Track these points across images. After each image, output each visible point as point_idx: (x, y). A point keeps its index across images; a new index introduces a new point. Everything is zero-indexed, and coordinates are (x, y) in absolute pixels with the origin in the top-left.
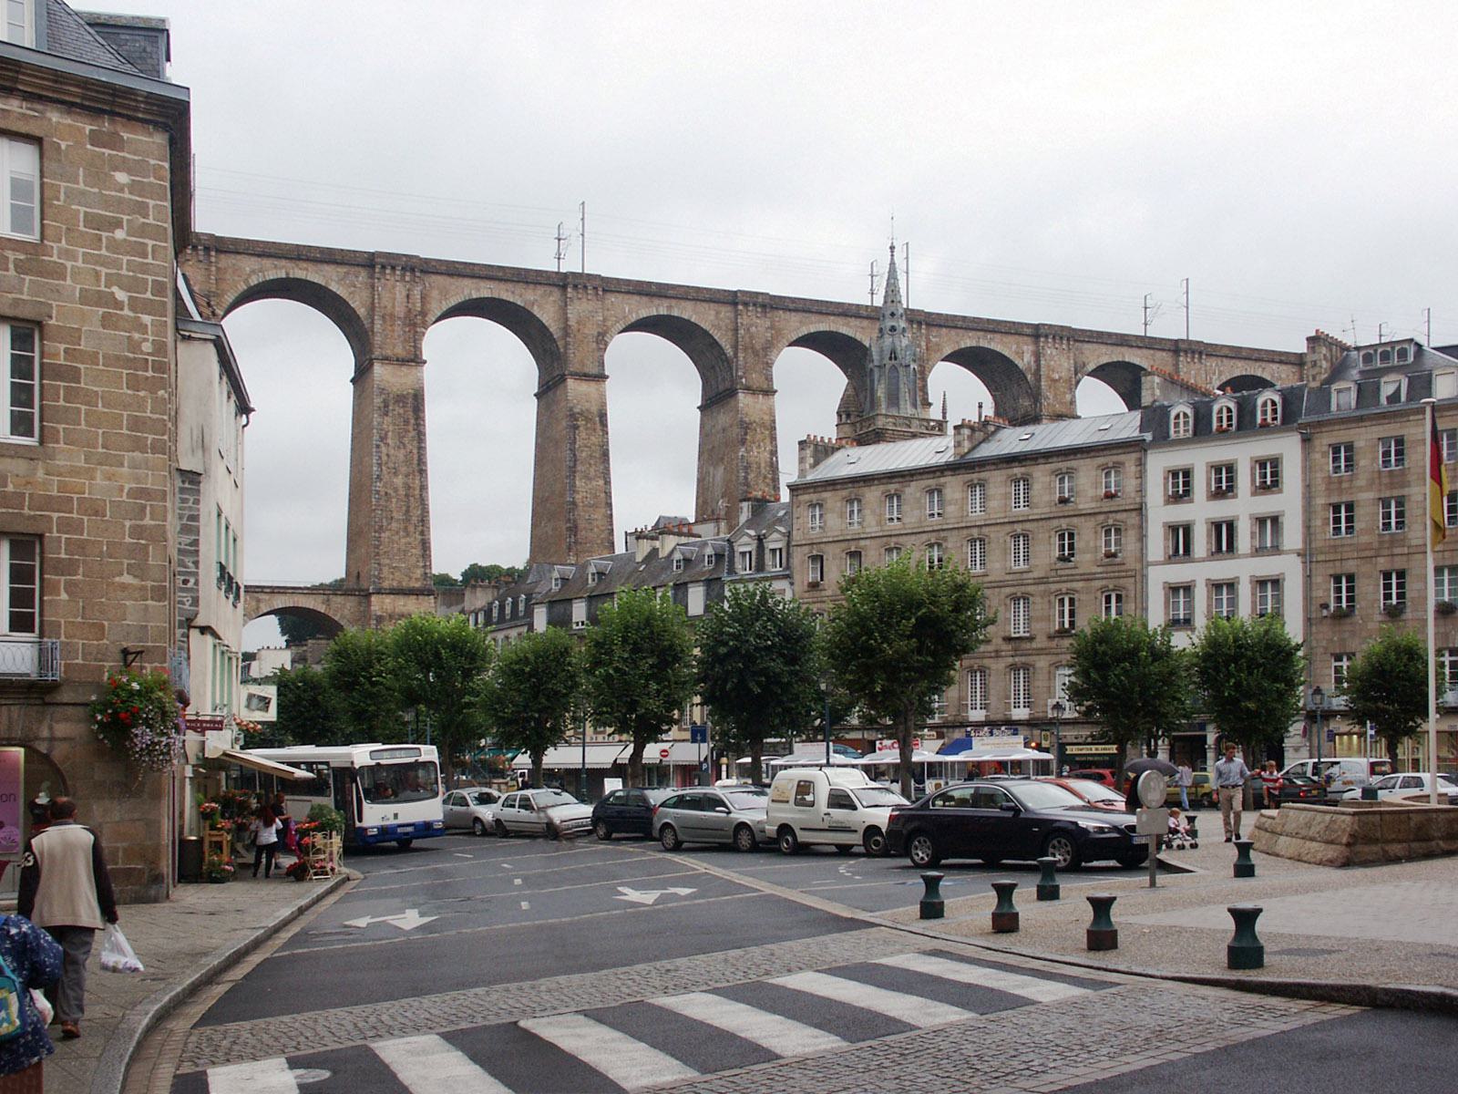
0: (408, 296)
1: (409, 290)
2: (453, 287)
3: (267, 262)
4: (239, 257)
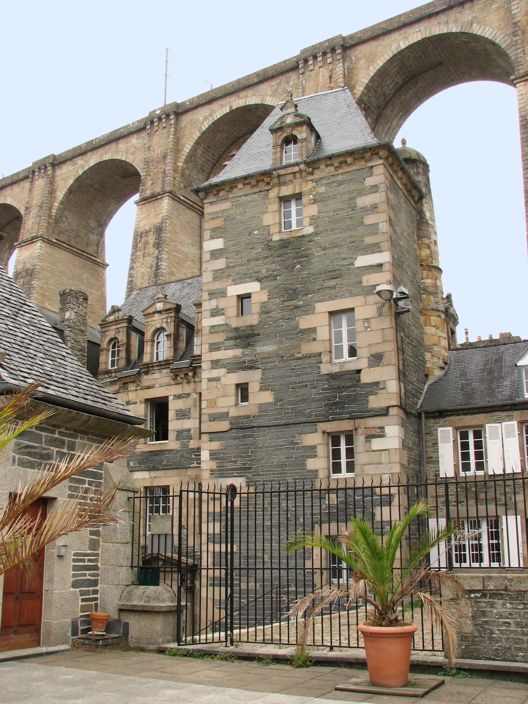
0: (330, 77)
1: (331, 71)
2: (380, 48)
3: (215, 106)
4: (195, 112)
